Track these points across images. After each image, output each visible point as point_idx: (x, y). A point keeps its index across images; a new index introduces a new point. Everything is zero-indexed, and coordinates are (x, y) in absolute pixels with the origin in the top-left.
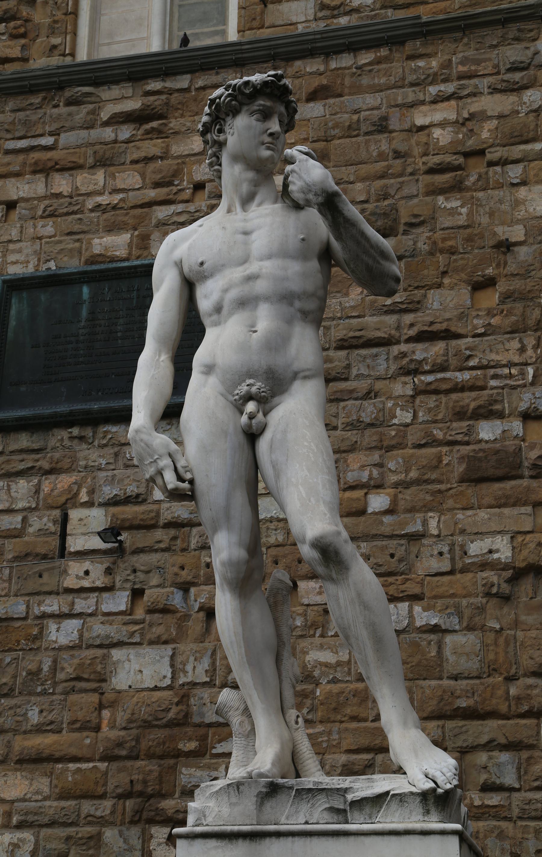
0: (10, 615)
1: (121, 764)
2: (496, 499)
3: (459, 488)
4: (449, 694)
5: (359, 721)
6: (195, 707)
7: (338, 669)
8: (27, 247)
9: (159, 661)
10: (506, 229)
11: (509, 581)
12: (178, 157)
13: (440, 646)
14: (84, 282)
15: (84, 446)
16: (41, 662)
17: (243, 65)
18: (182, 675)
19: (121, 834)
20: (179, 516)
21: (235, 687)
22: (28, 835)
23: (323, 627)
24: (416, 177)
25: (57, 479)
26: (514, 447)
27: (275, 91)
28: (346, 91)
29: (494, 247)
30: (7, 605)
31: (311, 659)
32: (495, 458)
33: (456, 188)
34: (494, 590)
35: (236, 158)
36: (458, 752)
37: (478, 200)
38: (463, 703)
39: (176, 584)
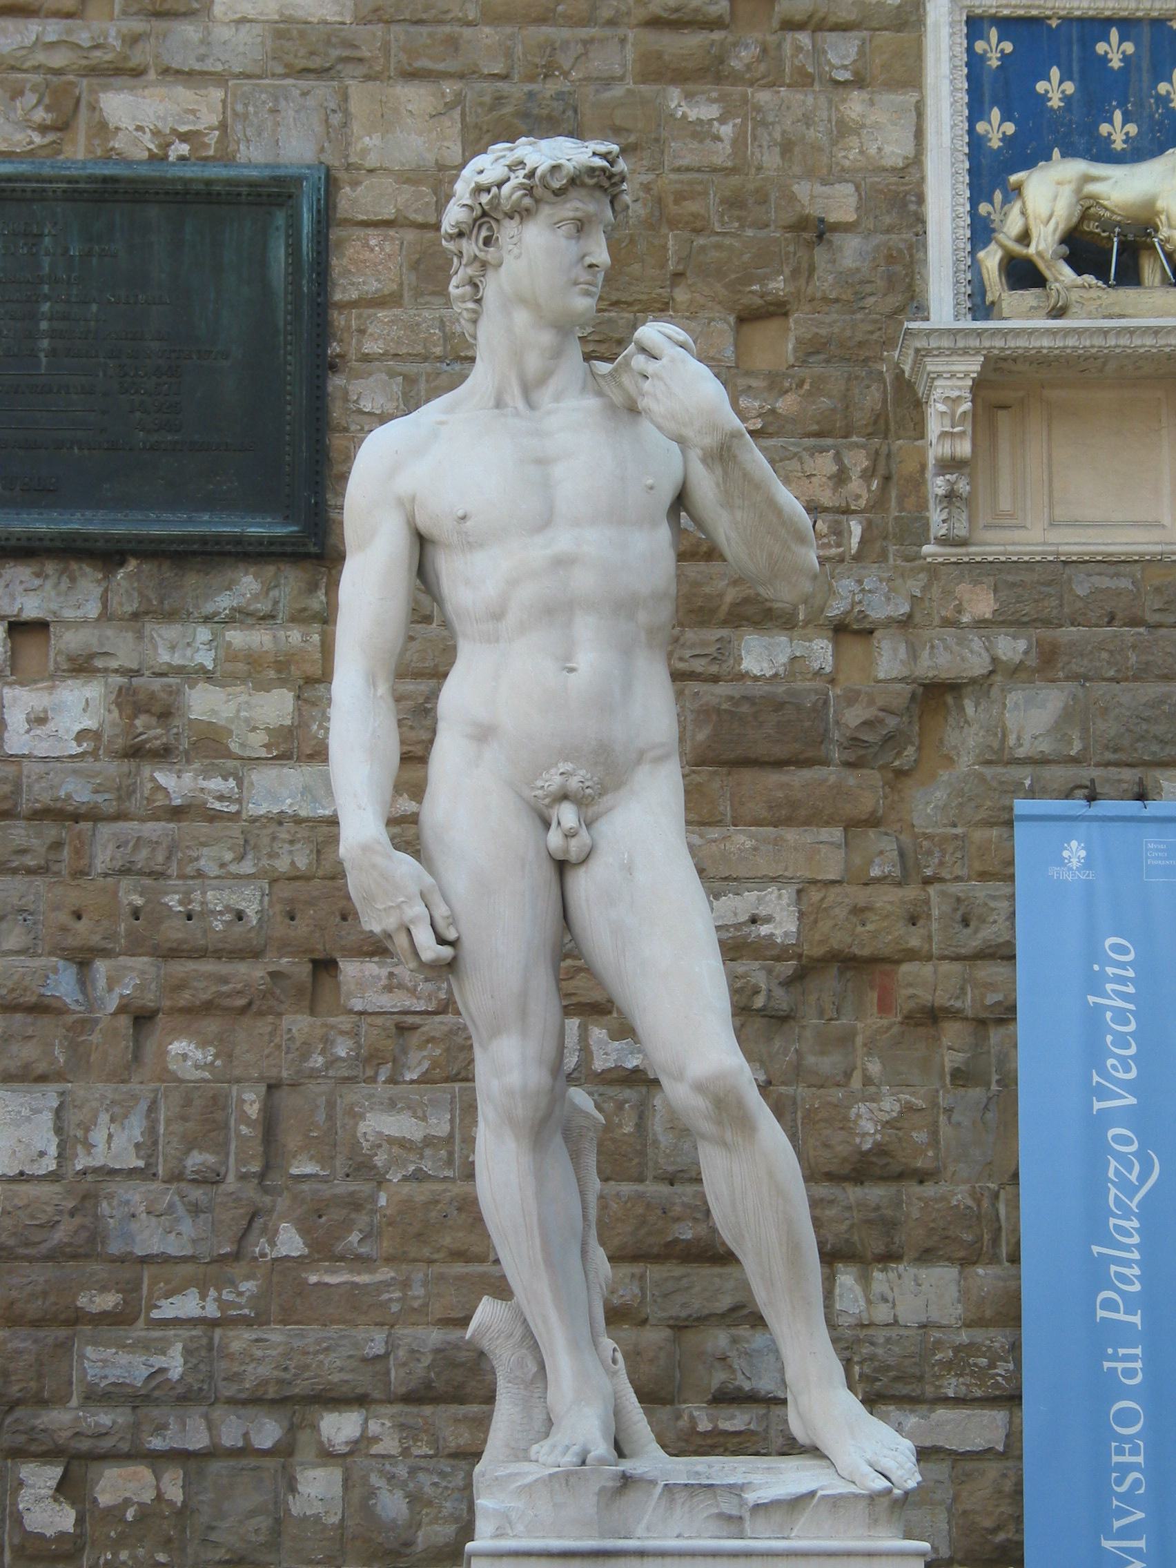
2: (771, 808)
3: (694, 776)
4: (659, 1212)
5: (468, 1260)
6: (111, 1221)
7: (428, 1152)
9: (28, 1119)
10: (819, 189)
11: (788, 983)
18: (80, 1149)
20: (69, 797)
23: (395, 1061)
24: (621, 32)
26: (814, 698)
29: (790, 228)
31: (368, 1130)
33: (710, 72)
34: (759, 1002)
36: (669, 1326)
37: (758, 109)
39: (64, 949)
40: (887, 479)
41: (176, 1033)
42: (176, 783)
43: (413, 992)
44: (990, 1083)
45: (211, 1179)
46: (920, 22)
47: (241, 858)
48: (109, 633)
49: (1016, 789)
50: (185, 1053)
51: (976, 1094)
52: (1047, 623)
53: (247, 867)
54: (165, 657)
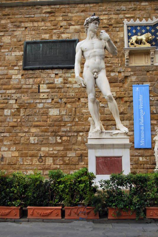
0: (31, 102)
1: (51, 127)
8: (30, 36)
12: (57, 21)
13: (104, 109)
15: (42, 73)
17: (69, 4)
19: (52, 138)
21: (91, 117)
22: (36, 138)
27: (98, 19)
28: (88, 11)
32: (113, 79)
35: (91, 30)
37: (111, 33)
38: (108, 119)
40: (122, 61)
41: (68, 104)
42: (68, 85)
43: (86, 101)
44: (131, 107)
45: (71, 115)
46: (124, 27)
47: (73, 91)
48: (63, 74)
49: (133, 84)
50: (69, 106)
51: (130, 107)
52: (135, 71)
53: (73, 91)
54: (67, 76)
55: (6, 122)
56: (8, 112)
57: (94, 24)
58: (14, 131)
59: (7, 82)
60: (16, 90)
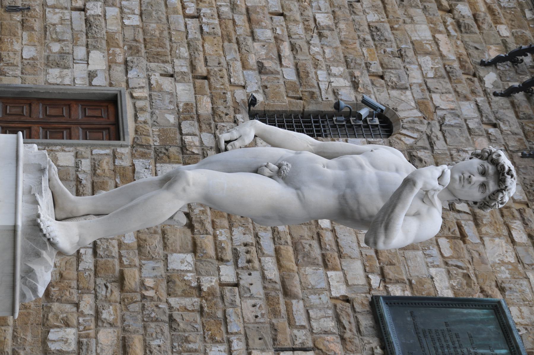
14: (510, 350)
16: (195, 342)
25: (338, 343)
30: (236, 322)
55: (140, 259)
56: (182, 262)
57: (481, 168)
58: (100, 281)
59: (307, 255)
60: (278, 280)
